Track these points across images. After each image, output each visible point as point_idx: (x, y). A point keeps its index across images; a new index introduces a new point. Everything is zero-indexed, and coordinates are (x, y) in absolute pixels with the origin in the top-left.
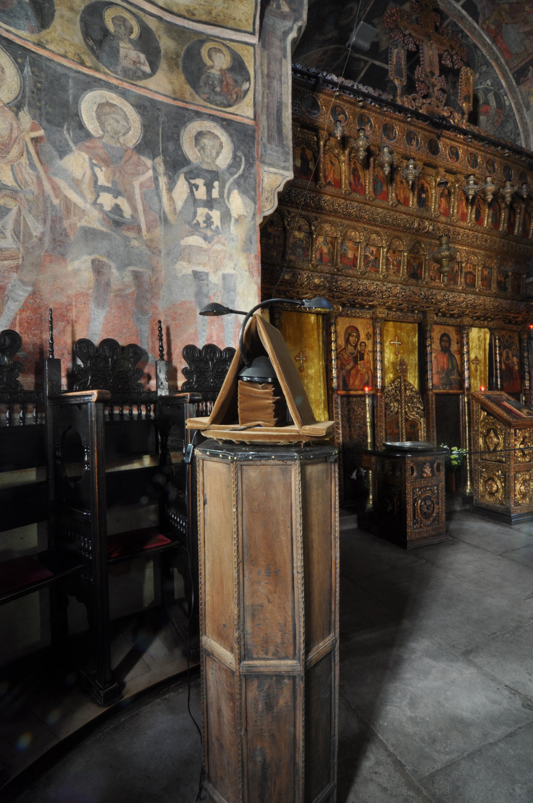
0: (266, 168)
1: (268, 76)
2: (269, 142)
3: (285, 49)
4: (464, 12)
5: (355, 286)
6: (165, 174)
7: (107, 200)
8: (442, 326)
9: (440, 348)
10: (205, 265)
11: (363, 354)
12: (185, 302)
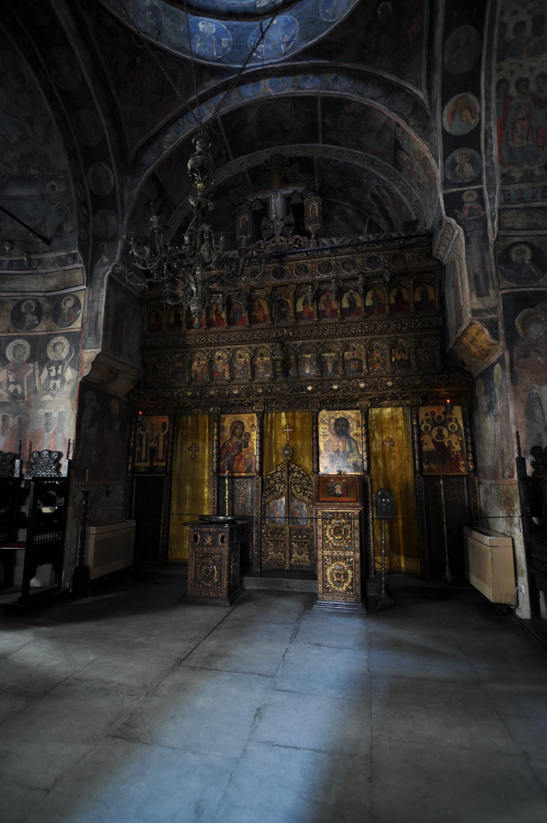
0: (86, 351)
1: (93, 301)
2: (89, 336)
3: (103, 283)
4: (328, 146)
5: (222, 392)
6: (39, 368)
7: (12, 388)
8: (337, 412)
9: (334, 433)
10: (51, 409)
11: (247, 443)
12: (40, 429)
